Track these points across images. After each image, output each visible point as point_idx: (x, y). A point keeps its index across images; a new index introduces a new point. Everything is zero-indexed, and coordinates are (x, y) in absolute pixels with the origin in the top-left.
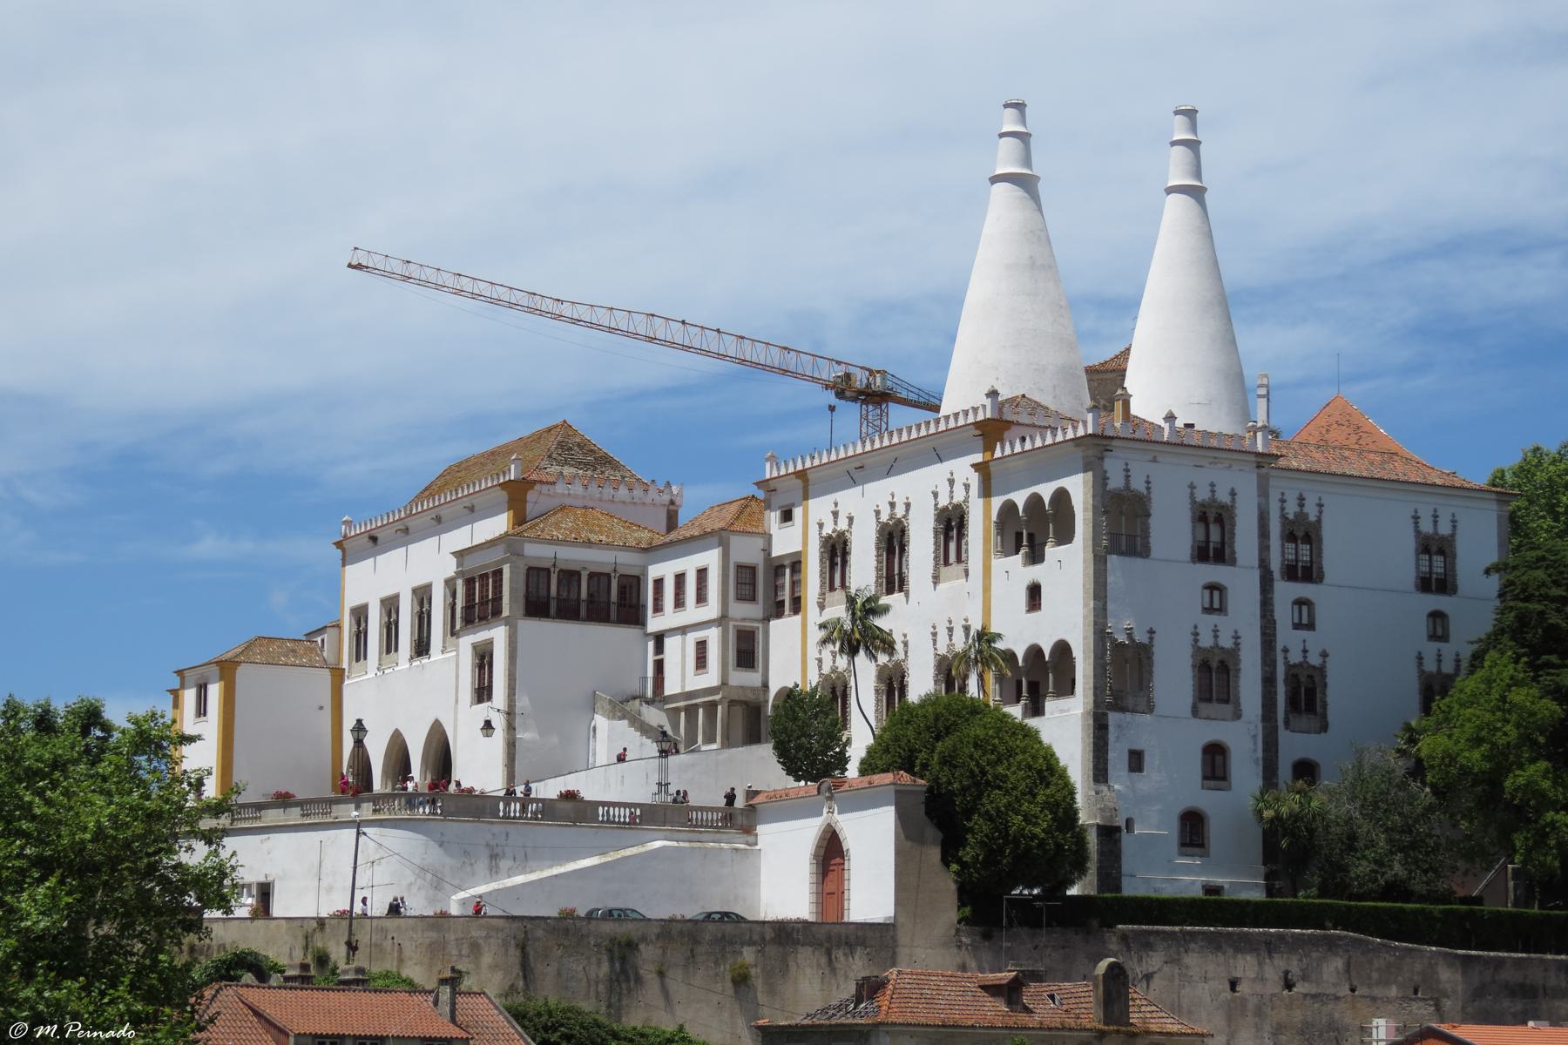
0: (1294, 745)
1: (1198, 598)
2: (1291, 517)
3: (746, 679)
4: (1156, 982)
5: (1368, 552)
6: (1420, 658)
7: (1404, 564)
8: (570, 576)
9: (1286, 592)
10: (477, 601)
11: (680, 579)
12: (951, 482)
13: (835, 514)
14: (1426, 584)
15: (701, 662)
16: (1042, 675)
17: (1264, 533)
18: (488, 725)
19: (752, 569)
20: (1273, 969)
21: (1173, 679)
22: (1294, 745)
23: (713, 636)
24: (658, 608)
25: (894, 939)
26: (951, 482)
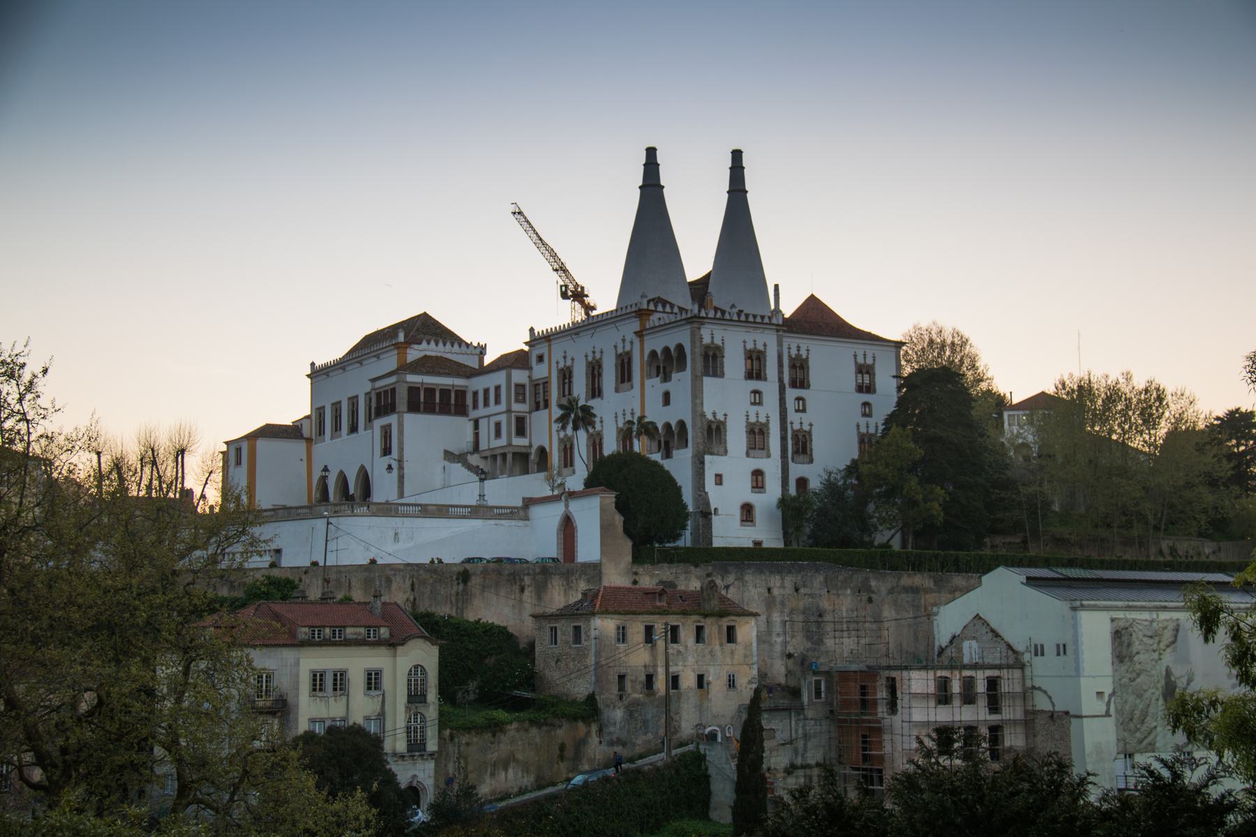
0: (797, 470)
1: (748, 398)
3: (519, 442)
4: (731, 590)
5: (984, 386)
6: (858, 426)
7: (849, 379)
8: (430, 391)
9: (791, 394)
10: (384, 404)
11: (486, 391)
12: (624, 340)
13: (565, 357)
14: (860, 389)
15: (498, 434)
16: (672, 438)
17: (780, 365)
18: (390, 468)
19: (523, 386)
20: (789, 581)
21: (736, 438)
22: (797, 470)
23: (503, 419)
24: (475, 406)
25: (601, 572)
26: (624, 340)
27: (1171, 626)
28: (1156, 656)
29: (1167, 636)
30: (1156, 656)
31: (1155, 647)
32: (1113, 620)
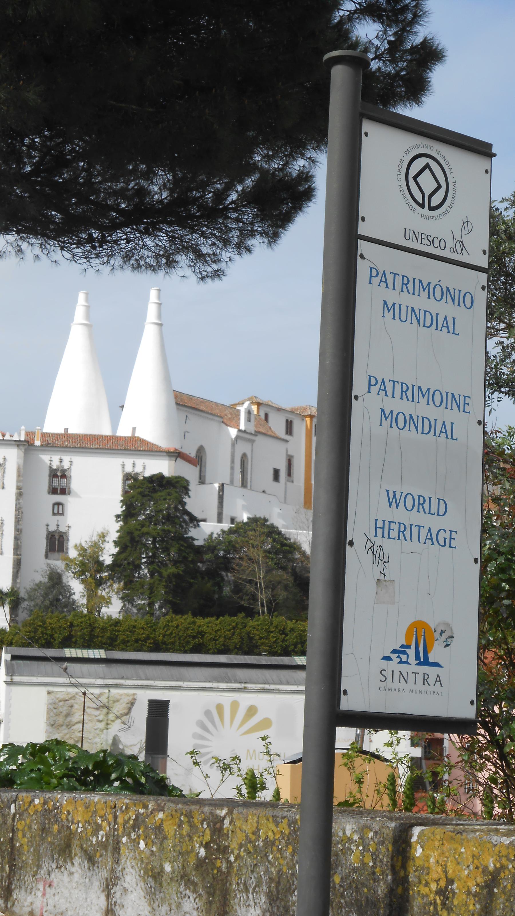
2: (54, 467)
27: (125, 700)
28: (102, 725)
29: (118, 708)
30: (102, 725)
31: (101, 717)
32: (49, 693)
